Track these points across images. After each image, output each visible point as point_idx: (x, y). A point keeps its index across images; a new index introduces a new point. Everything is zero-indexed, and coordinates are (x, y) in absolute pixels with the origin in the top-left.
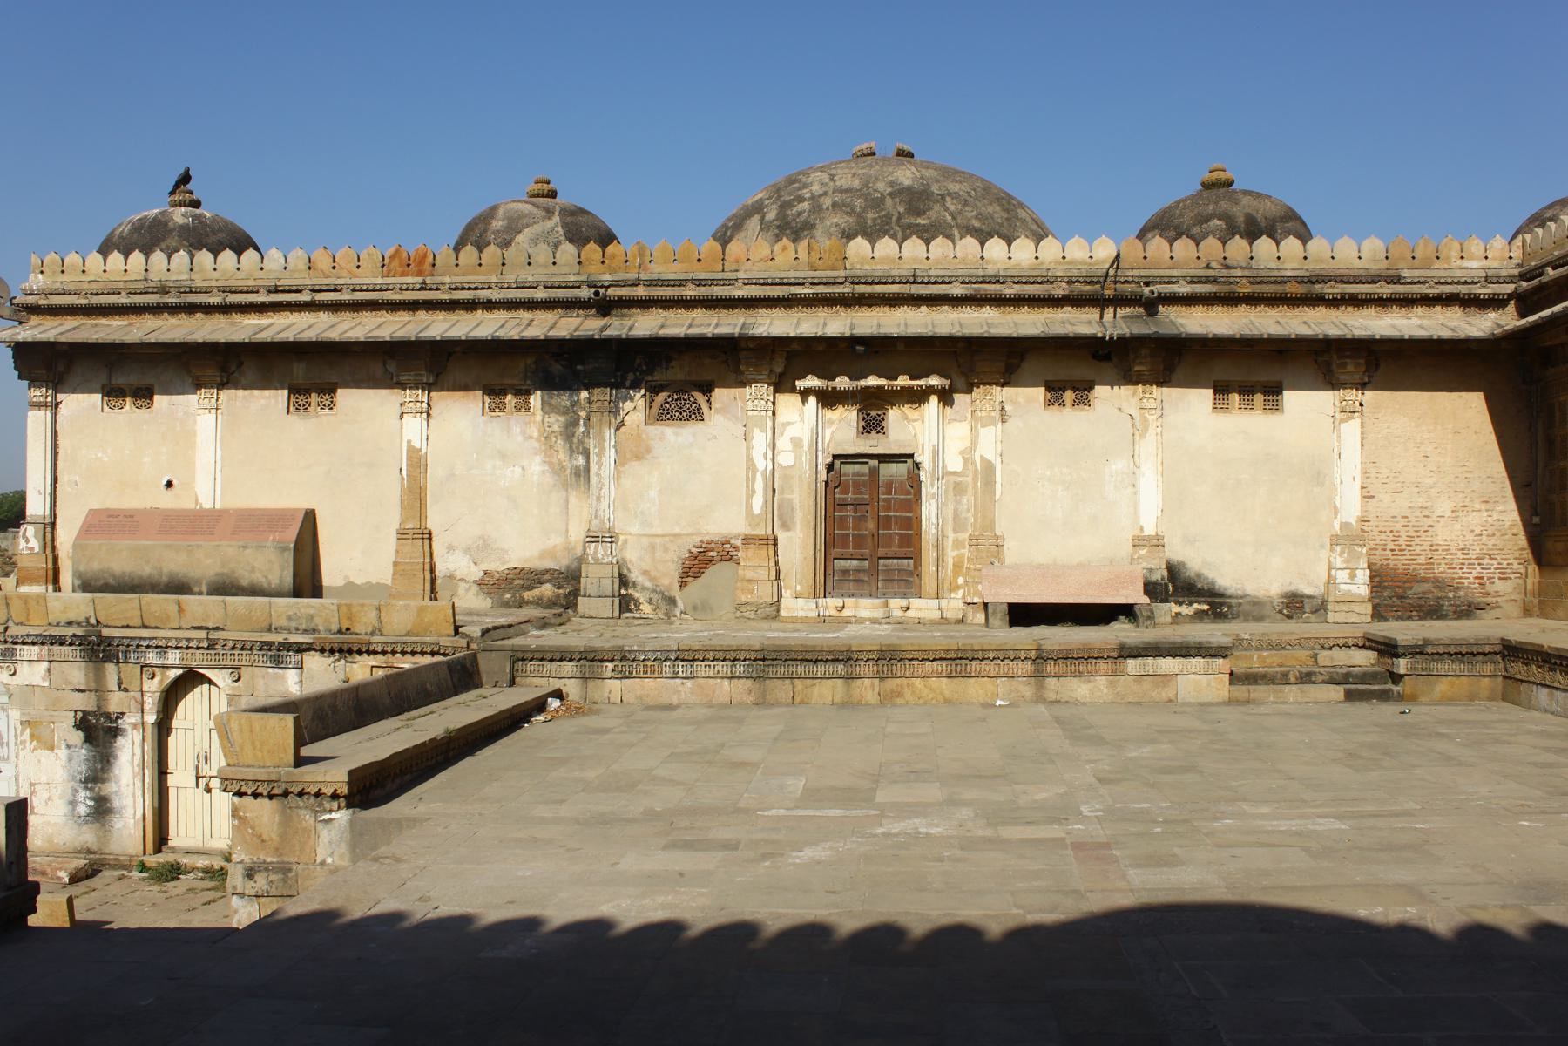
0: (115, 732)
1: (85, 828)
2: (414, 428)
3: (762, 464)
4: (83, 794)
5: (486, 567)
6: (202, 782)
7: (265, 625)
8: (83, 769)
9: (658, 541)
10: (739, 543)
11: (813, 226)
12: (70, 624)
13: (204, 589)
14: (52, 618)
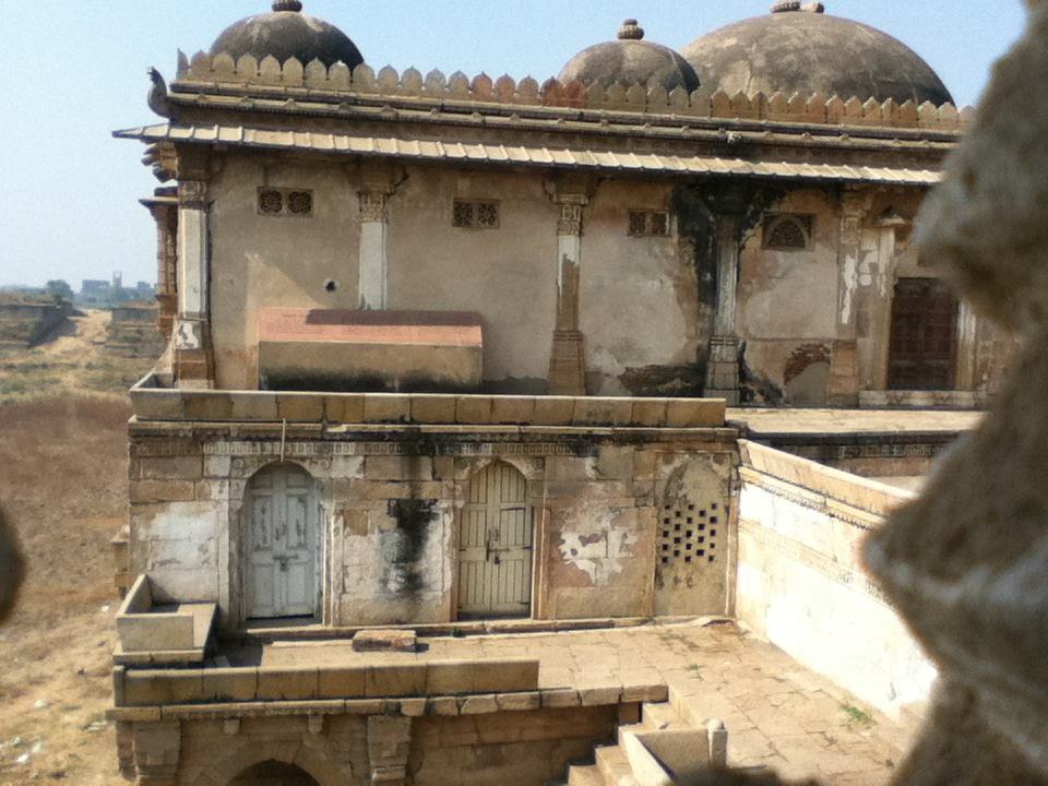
0: (431, 516)
1: (395, 602)
2: (569, 246)
3: (851, 284)
4: (394, 573)
5: (629, 364)
6: (492, 555)
7: (568, 419)
8: (393, 551)
9: (770, 345)
10: (830, 346)
11: (805, 77)
12: (384, 422)
13: (397, 384)
14: (367, 416)
